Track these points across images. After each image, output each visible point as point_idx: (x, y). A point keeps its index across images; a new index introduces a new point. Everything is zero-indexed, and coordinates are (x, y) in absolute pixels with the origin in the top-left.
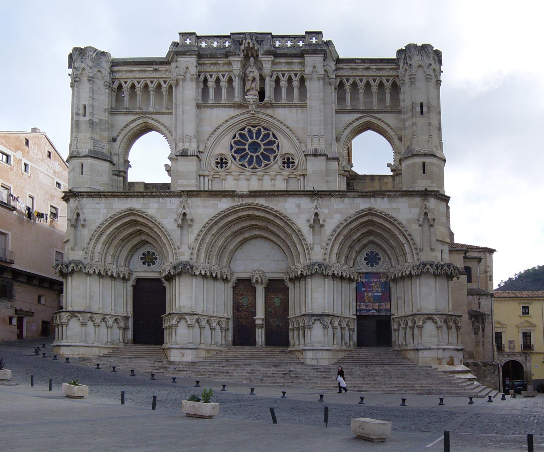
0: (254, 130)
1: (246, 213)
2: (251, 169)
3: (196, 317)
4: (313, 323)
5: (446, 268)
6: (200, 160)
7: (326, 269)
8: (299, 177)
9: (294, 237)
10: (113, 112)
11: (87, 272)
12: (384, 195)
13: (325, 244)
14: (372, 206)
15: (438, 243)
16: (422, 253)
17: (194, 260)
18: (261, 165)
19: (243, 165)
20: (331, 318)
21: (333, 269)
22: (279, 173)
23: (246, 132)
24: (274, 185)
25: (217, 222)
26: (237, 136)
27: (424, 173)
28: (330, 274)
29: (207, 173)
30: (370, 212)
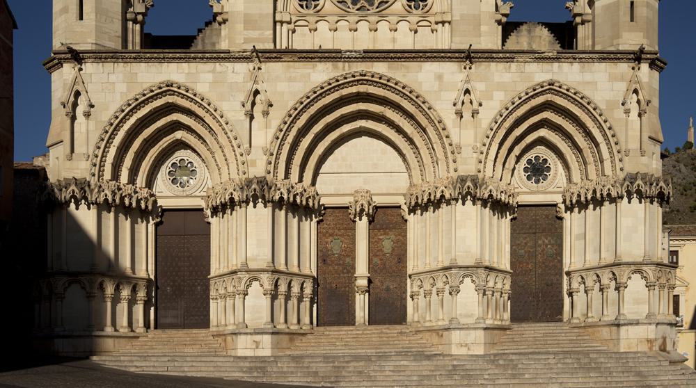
1: (354, 90)
2: (358, 10)
4: (462, 282)
8: (435, 27)
9: (430, 130)
11: (94, 199)
12: (575, 59)
13: (478, 145)
14: (555, 78)
15: (651, 142)
18: (372, 5)
21: (490, 187)
22: (402, 18)
24: (394, 40)
27: (632, 20)
28: (486, 196)
30: (552, 88)
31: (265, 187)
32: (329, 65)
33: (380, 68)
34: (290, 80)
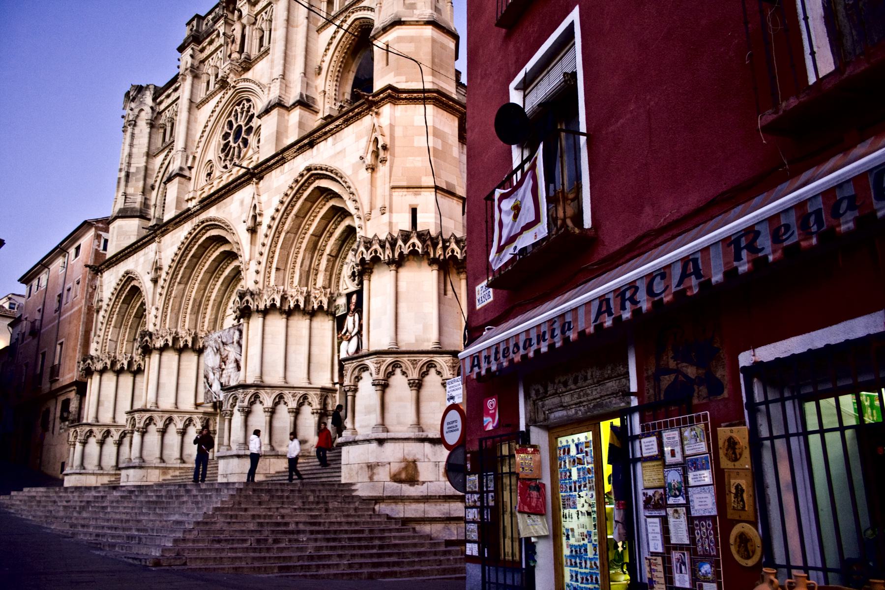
0: (239, 109)
3: (148, 415)
5: (400, 242)
6: (190, 179)
7: (253, 299)
10: (149, 155)
16: (368, 223)
17: (158, 327)
19: (225, 167)
20: (252, 391)
23: (232, 118)
25: (180, 262)
26: (226, 127)
27: (387, 64)
28: (262, 307)
29: (191, 196)
31: (147, 338)
32: (189, 222)
33: (212, 212)
34: (172, 245)
